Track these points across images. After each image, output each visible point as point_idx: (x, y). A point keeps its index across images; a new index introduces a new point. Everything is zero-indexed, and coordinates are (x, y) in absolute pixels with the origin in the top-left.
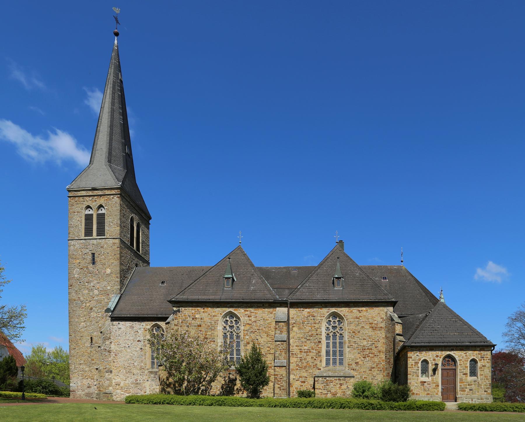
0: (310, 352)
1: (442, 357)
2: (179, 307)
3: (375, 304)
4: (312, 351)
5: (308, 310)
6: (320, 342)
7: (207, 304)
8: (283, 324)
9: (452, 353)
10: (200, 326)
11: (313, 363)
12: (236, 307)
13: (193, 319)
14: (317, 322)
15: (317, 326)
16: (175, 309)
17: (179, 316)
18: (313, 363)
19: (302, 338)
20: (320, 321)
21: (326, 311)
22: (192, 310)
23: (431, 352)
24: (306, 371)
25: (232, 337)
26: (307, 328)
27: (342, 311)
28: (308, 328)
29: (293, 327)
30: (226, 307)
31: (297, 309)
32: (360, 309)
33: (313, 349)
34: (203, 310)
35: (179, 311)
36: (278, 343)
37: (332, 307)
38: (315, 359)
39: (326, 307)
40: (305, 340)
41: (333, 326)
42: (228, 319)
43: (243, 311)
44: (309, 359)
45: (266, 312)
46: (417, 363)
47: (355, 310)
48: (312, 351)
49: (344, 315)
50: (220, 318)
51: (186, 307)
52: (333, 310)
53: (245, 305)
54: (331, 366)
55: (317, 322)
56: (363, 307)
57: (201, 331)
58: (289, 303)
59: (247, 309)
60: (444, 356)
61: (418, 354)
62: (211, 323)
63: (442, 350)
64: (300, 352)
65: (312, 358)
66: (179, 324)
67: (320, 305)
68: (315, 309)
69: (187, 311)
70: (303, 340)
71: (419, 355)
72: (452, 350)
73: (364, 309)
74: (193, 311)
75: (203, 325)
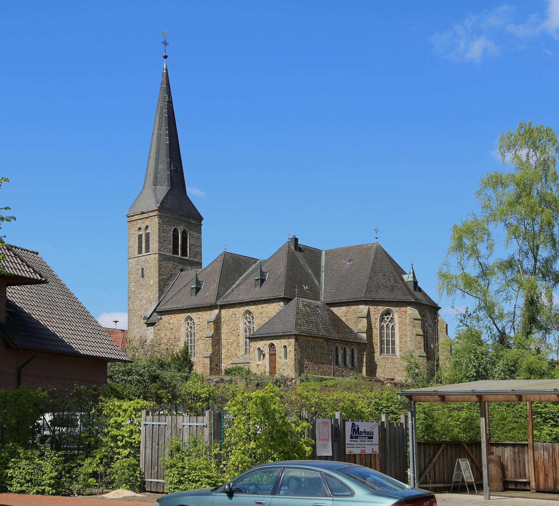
0: (233, 344)
1: (268, 345)
2: (161, 315)
3: (272, 301)
4: (234, 342)
5: (232, 310)
6: (239, 335)
7: (176, 312)
8: (211, 323)
9: (273, 342)
10: (172, 329)
11: (235, 352)
12: (192, 312)
13: (169, 324)
14: (237, 319)
15: (237, 322)
16: (159, 317)
17: (161, 323)
18: (235, 352)
19: (228, 333)
20: (239, 318)
21: (242, 310)
22: (168, 317)
23: (261, 342)
24: (231, 359)
25: (191, 336)
26: (231, 324)
27: (252, 308)
28: (232, 324)
29: (223, 324)
30: (186, 313)
31: (226, 310)
32: (263, 306)
33: (235, 341)
34: (174, 316)
35: (161, 319)
36: (207, 339)
37: (246, 305)
38: (236, 350)
39: (242, 306)
40: (230, 334)
41: (249, 322)
42: (189, 321)
43: (195, 314)
44: (232, 350)
45: (208, 314)
46: (254, 350)
47: (259, 306)
48: (234, 342)
49: (253, 312)
50: (183, 321)
51: (165, 315)
52: (247, 308)
53: (196, 310)
54: (247, 355)
55: (237, 319)
56: (265, 304)
57: (172, 333)
58: (219, 306)
59: (198, 313)
60: (269, 344)
61: (255, 343)
62: (178, 326)
63: (267, 340)
64: (228, 344)
65: (234, 348)
66: (161, 329)
67: (238, 305)
68: (236, 309)
69: (166, 318)
70: (229, 334)
71: (256, 344)
72: (273, 339)
73: (265, 305)
74: (169, 318)
75: (174, 328)
